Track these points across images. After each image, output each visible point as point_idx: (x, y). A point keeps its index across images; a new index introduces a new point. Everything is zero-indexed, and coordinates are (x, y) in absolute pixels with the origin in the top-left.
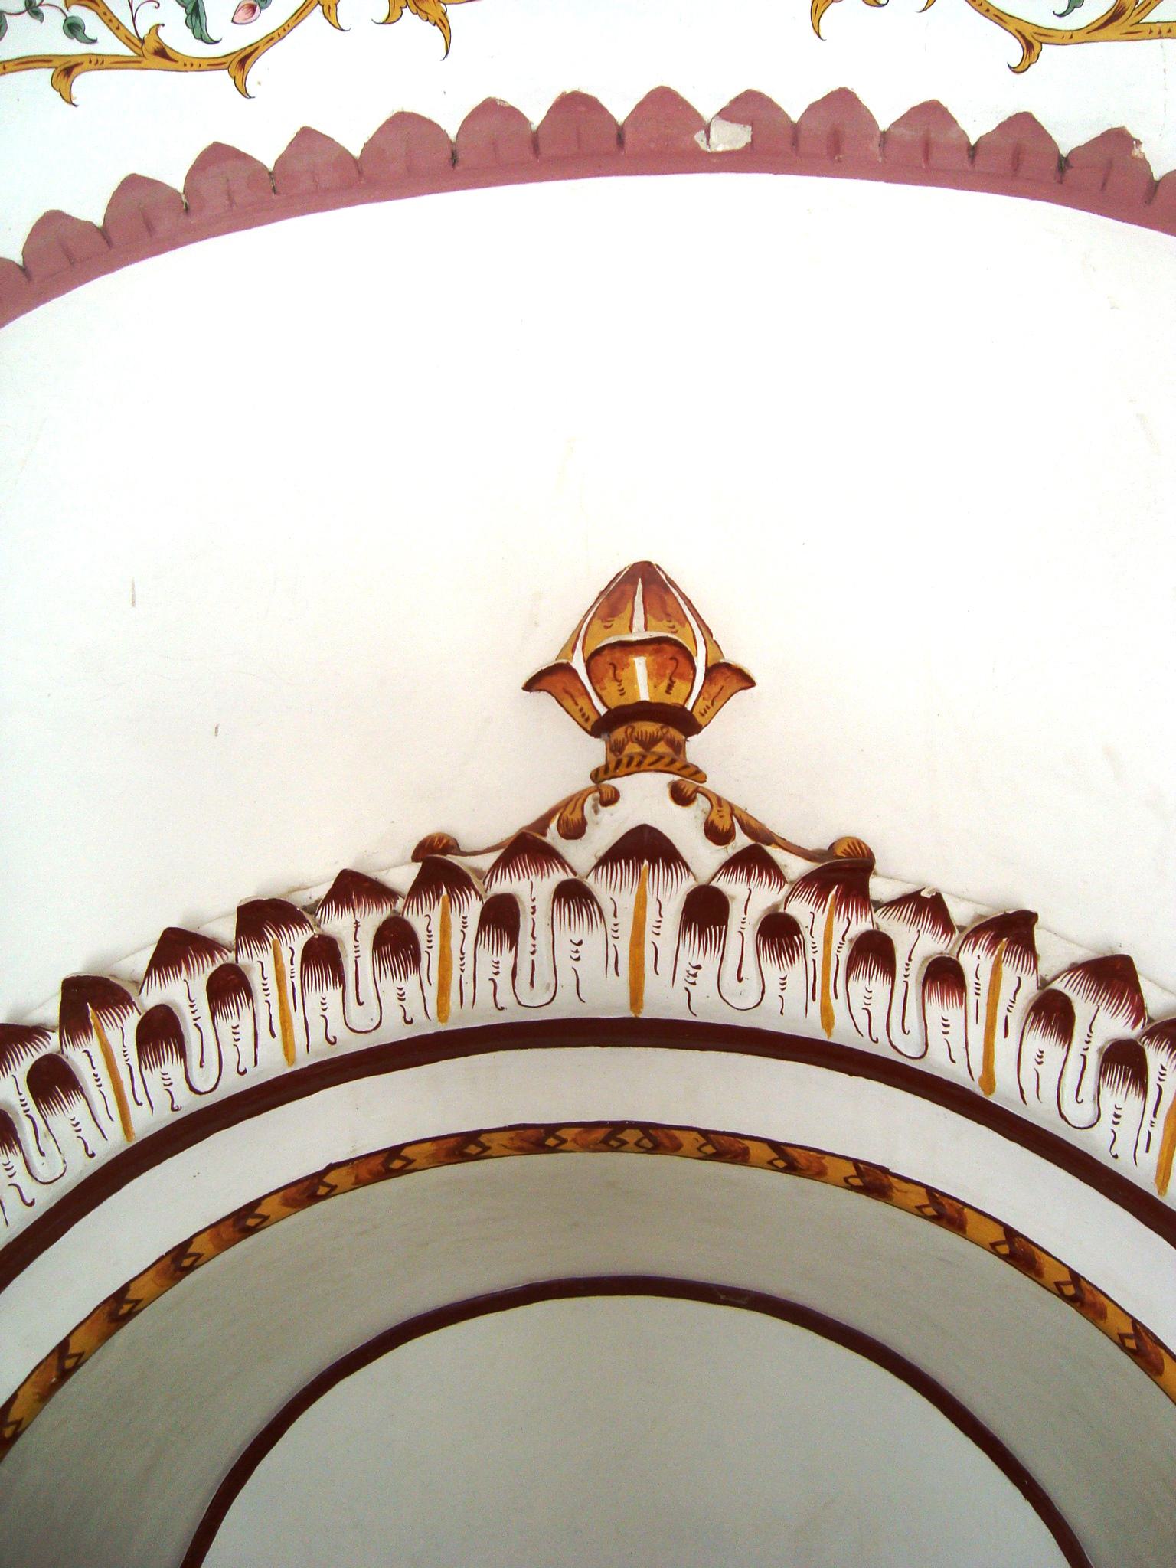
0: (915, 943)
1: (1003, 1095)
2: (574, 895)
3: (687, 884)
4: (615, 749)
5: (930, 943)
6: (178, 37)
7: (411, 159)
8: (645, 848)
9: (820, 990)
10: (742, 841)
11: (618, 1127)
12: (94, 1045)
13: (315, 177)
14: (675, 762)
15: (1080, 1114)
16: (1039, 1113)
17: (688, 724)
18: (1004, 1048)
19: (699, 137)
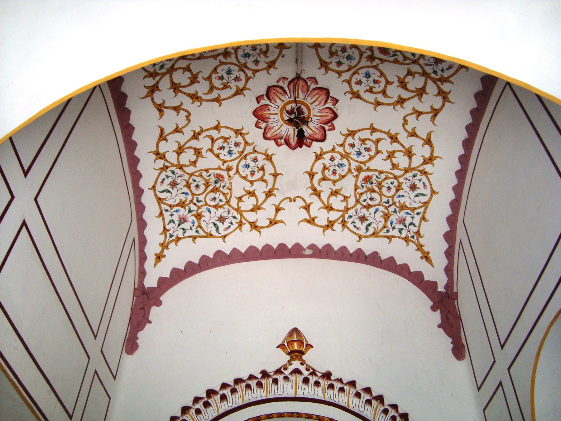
0: (338, 385)
1: (351, 408)
2: (286, 378)
3: (303, 377)
4: (291, 357)
5: (340, 385)
6: (214, 233)
7: (253, 254)
8: (297, 371)
9: (324, 392)
10: (311, 371)
11: (293, 413)
12: (213, 399)
13: (236, 257)
14: (301, 359)
15: (362, 410)
16: (356, 410)
17: (303, 353)
18: (351, 400)
19: (304, 252)
